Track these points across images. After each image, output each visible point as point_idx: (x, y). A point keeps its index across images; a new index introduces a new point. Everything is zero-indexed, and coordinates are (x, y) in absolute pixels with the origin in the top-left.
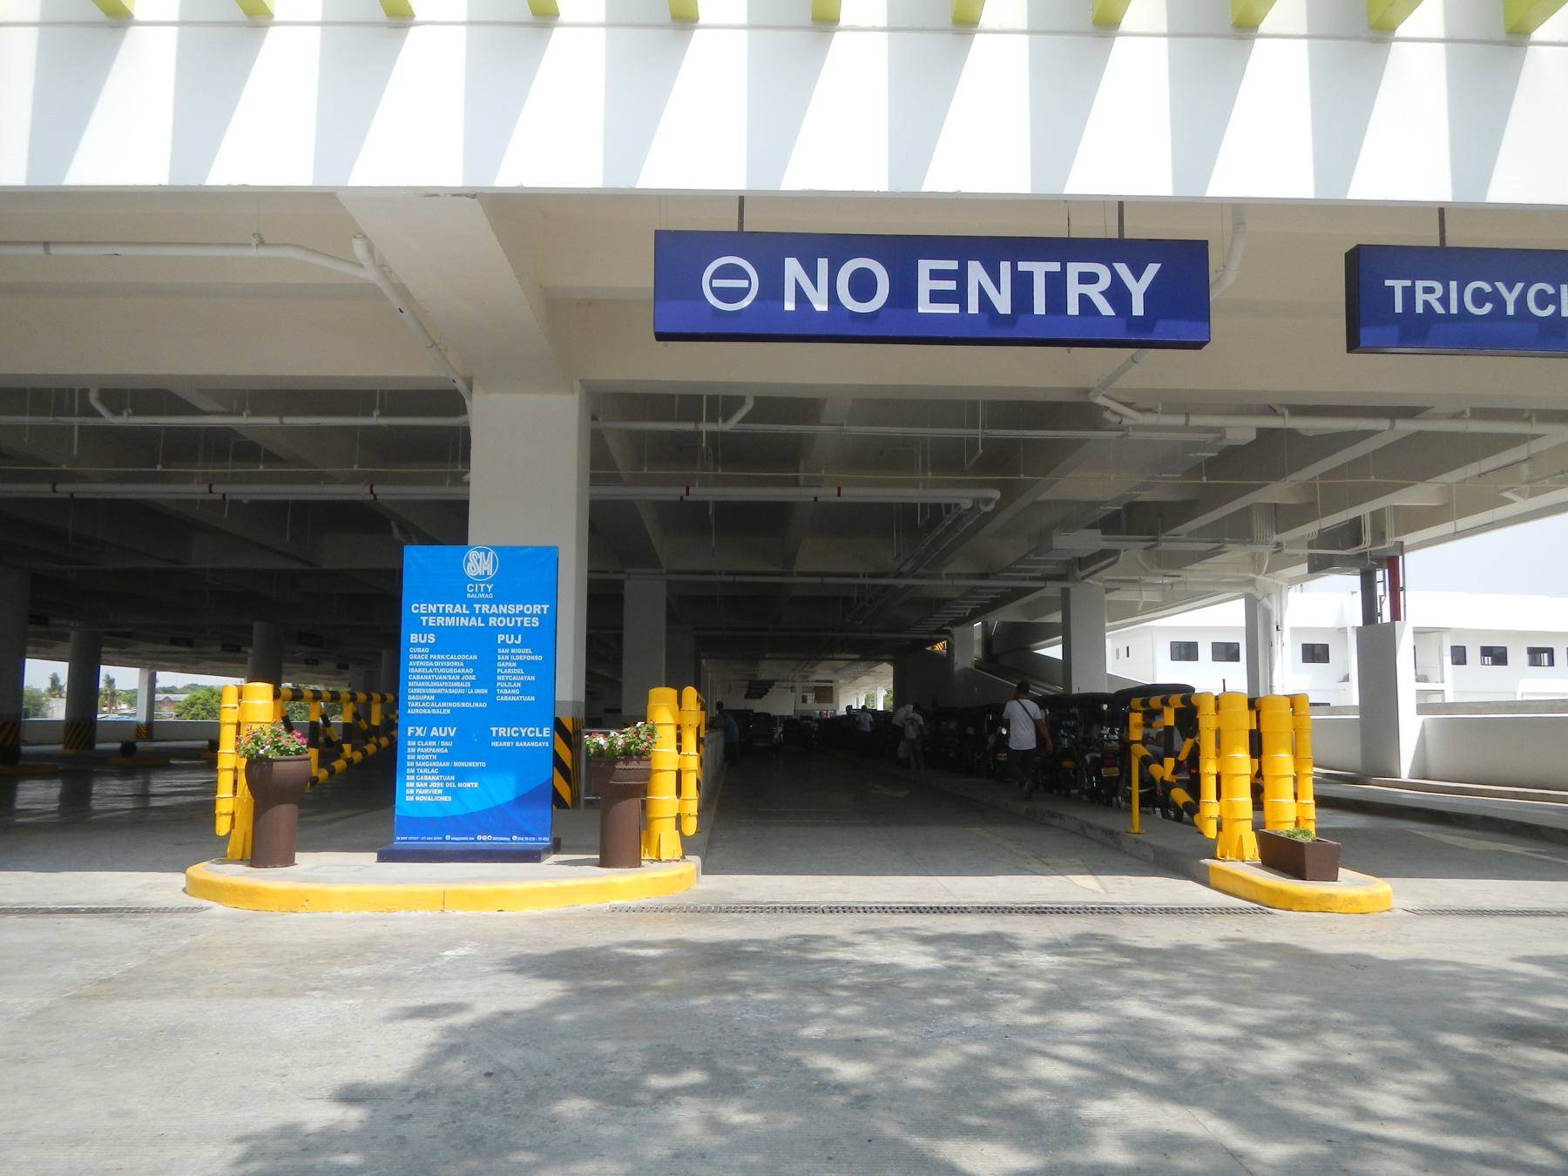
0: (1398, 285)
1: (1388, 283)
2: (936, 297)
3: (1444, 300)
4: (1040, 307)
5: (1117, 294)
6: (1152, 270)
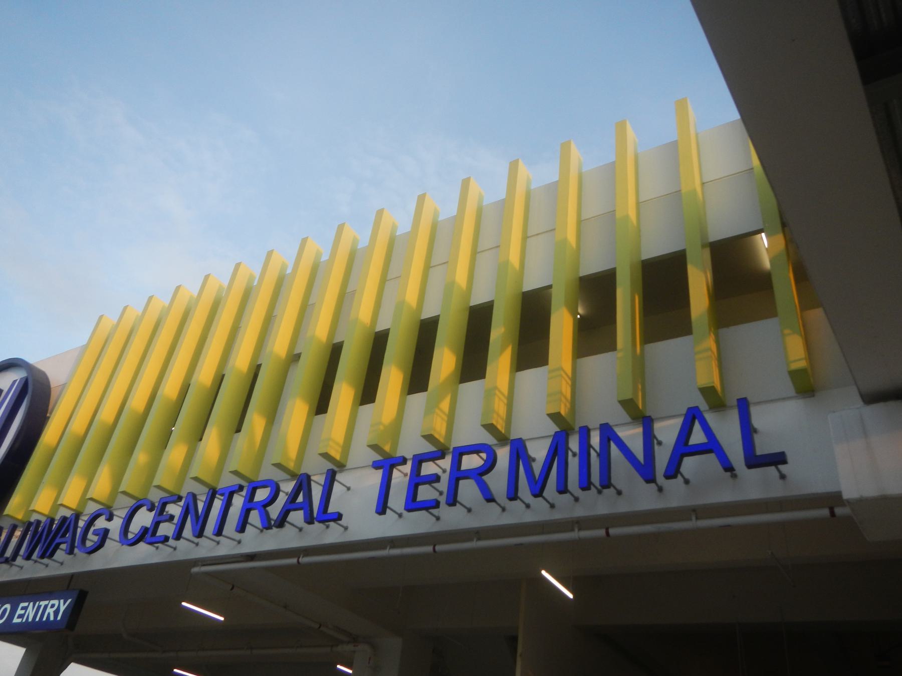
2: (21, 616)
4: (37, 619)
5: (56, 613)
6: (69, 601)
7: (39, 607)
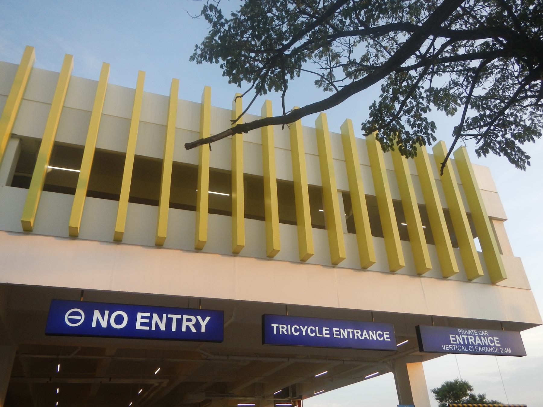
0: (275, 326)
1: (272, 325)
2: (142, 324)
3: (287, 330)
4: (174, 329)
5: (197, 325)
6: (208, 318)
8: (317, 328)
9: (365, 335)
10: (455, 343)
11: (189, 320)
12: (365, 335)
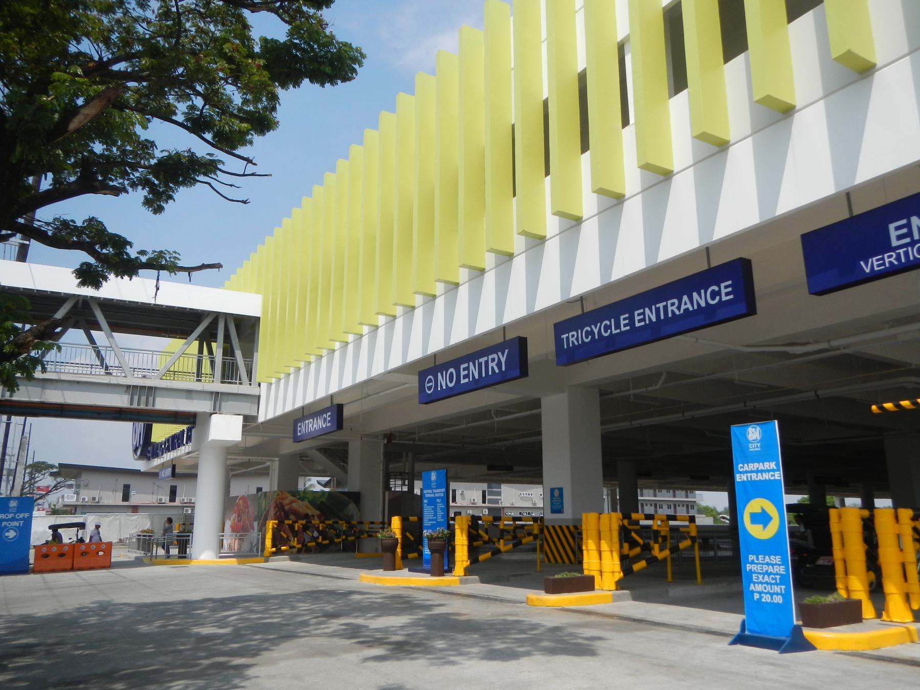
0: (564, 336)
2: (465, 377)
4: (484, 375)
5: (499, 364)
7: (480, 364)
8: (613, 320)
9: (686, 304)
10: (908, 240)
11: (493, 360)
12: (686, 304)
